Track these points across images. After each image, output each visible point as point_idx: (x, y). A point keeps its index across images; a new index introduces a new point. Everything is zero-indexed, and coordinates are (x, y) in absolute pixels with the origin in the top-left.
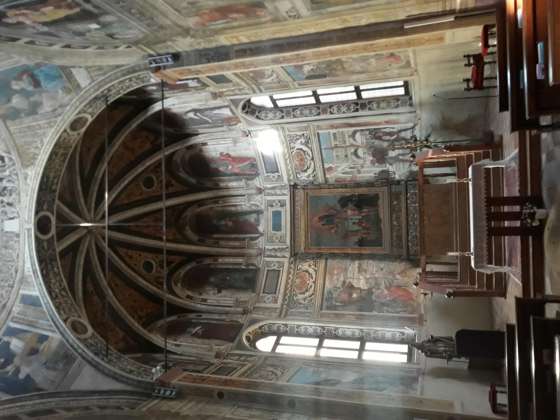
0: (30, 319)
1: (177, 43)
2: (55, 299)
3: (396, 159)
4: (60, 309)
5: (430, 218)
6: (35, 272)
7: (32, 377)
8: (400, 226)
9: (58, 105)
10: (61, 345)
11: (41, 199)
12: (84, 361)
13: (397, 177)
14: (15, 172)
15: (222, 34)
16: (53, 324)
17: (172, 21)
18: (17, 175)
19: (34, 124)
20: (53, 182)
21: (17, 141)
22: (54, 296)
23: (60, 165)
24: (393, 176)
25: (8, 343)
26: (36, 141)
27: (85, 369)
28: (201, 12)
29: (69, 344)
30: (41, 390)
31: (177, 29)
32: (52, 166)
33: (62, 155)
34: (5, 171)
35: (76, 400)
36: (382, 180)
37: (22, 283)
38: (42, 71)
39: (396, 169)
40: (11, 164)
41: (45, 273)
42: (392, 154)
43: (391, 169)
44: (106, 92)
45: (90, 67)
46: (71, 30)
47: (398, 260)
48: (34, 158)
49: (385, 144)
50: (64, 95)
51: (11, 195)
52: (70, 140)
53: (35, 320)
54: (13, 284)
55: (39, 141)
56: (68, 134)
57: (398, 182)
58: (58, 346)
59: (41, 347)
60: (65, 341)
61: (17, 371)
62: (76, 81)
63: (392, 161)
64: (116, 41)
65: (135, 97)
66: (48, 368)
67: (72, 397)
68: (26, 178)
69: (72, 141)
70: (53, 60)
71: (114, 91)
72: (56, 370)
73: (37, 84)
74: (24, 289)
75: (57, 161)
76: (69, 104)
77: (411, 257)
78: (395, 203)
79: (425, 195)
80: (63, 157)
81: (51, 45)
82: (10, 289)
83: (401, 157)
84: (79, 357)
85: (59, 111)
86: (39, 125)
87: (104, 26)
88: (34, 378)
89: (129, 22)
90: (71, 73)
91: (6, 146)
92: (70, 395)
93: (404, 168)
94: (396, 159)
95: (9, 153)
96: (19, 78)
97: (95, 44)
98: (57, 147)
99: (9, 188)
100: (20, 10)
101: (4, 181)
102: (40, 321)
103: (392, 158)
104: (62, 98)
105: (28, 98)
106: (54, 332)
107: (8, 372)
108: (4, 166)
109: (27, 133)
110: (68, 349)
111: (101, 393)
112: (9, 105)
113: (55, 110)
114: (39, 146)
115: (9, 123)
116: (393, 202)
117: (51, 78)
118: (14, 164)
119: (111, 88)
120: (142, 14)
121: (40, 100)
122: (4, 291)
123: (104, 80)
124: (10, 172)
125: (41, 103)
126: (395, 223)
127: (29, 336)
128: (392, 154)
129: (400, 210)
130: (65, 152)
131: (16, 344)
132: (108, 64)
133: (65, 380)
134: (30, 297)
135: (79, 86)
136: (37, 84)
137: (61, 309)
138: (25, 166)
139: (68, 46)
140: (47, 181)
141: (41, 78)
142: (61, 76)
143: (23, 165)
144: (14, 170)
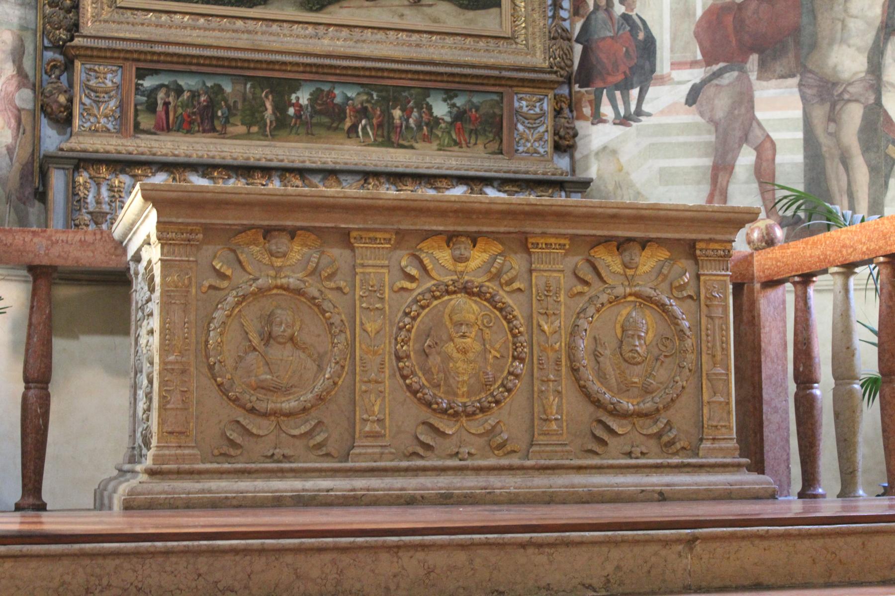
3: (735, 130)
5: (467, 290)
8: (282, 126)
13: (597, 136)
24: (606, 109)
36: (585, 37)
39: (663, 130)
42: (779, 107)
43: (665, 99)
47: (25, 98)
49: (848, 61)
57: (565, 143)
63: (721, 104)
77: (57, 180)
78: (441, 109)
79: (647, 262)
83: (746, 158)
93: (666, 177)
94: (735, 130)
103: (745, 100)
116: (449, 95)
126: (303, 97)
128: (779, 107)
129: (388, 135)
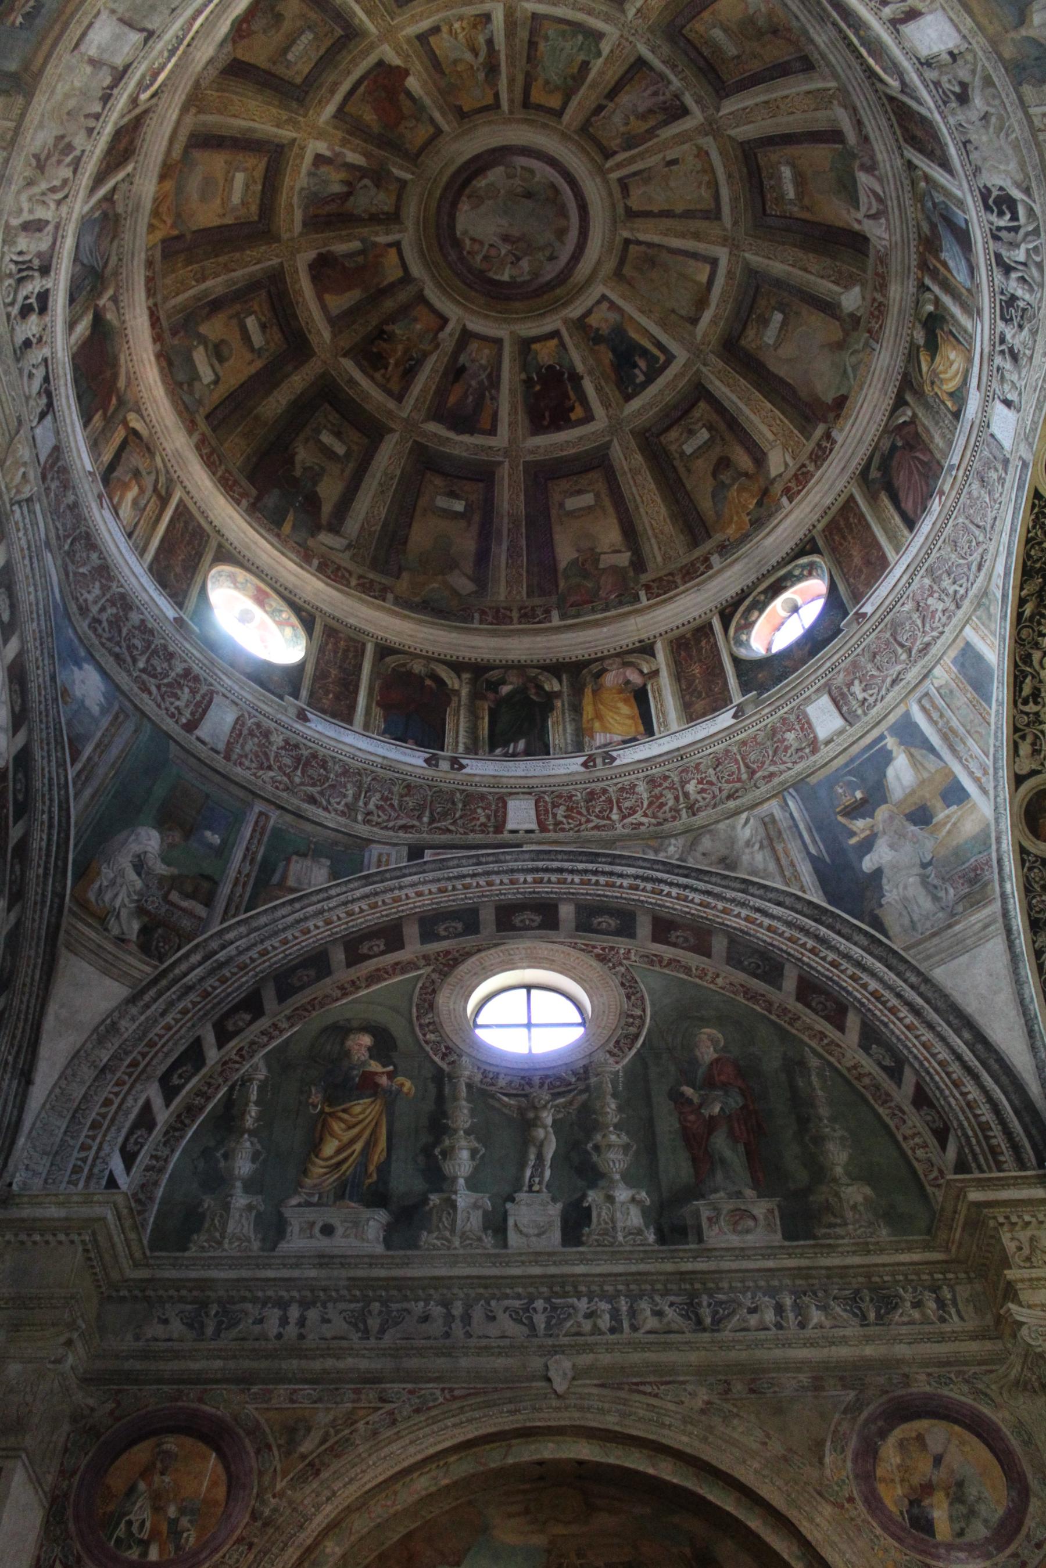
0: (955, 723)
2: (1025, 702)
4: (1023, 738)
6: (1005, 596)
7: (884, 881)
10: (983, 840)
12: (1000, 920)
16: (991, 771)
22: (1027, 690)
25: (887, 757)
27: (989, 945)
29: (998, 850)
30: (878, 924)
35: (917, 1012)
37: (979, 605)
40: (1030, 228)
41: (1027, 613)
53: (961, 730)
54: (963, 597)
58: (974, 838)
59: (941, 816)
60: (993, 835)
61: (867, 845)
66: (924, 881)
67: (921, 995)
72: (936, 899)
74: (975, 629)
82: (953, 607)
84: (996, 907)
88: (886, 888)
92: (923, 988)
102: (970, 742)
106: (985, 791)
107: (853, 834)
108: (1016, 229)
110: (988, 862)
111: (980, 1040)
122: (941, 606)
127: (932, 764)
131: (901, 773)
133: (935, 941)
134: (979, 658)
137: (1029, 739)
144: (1036, 249)
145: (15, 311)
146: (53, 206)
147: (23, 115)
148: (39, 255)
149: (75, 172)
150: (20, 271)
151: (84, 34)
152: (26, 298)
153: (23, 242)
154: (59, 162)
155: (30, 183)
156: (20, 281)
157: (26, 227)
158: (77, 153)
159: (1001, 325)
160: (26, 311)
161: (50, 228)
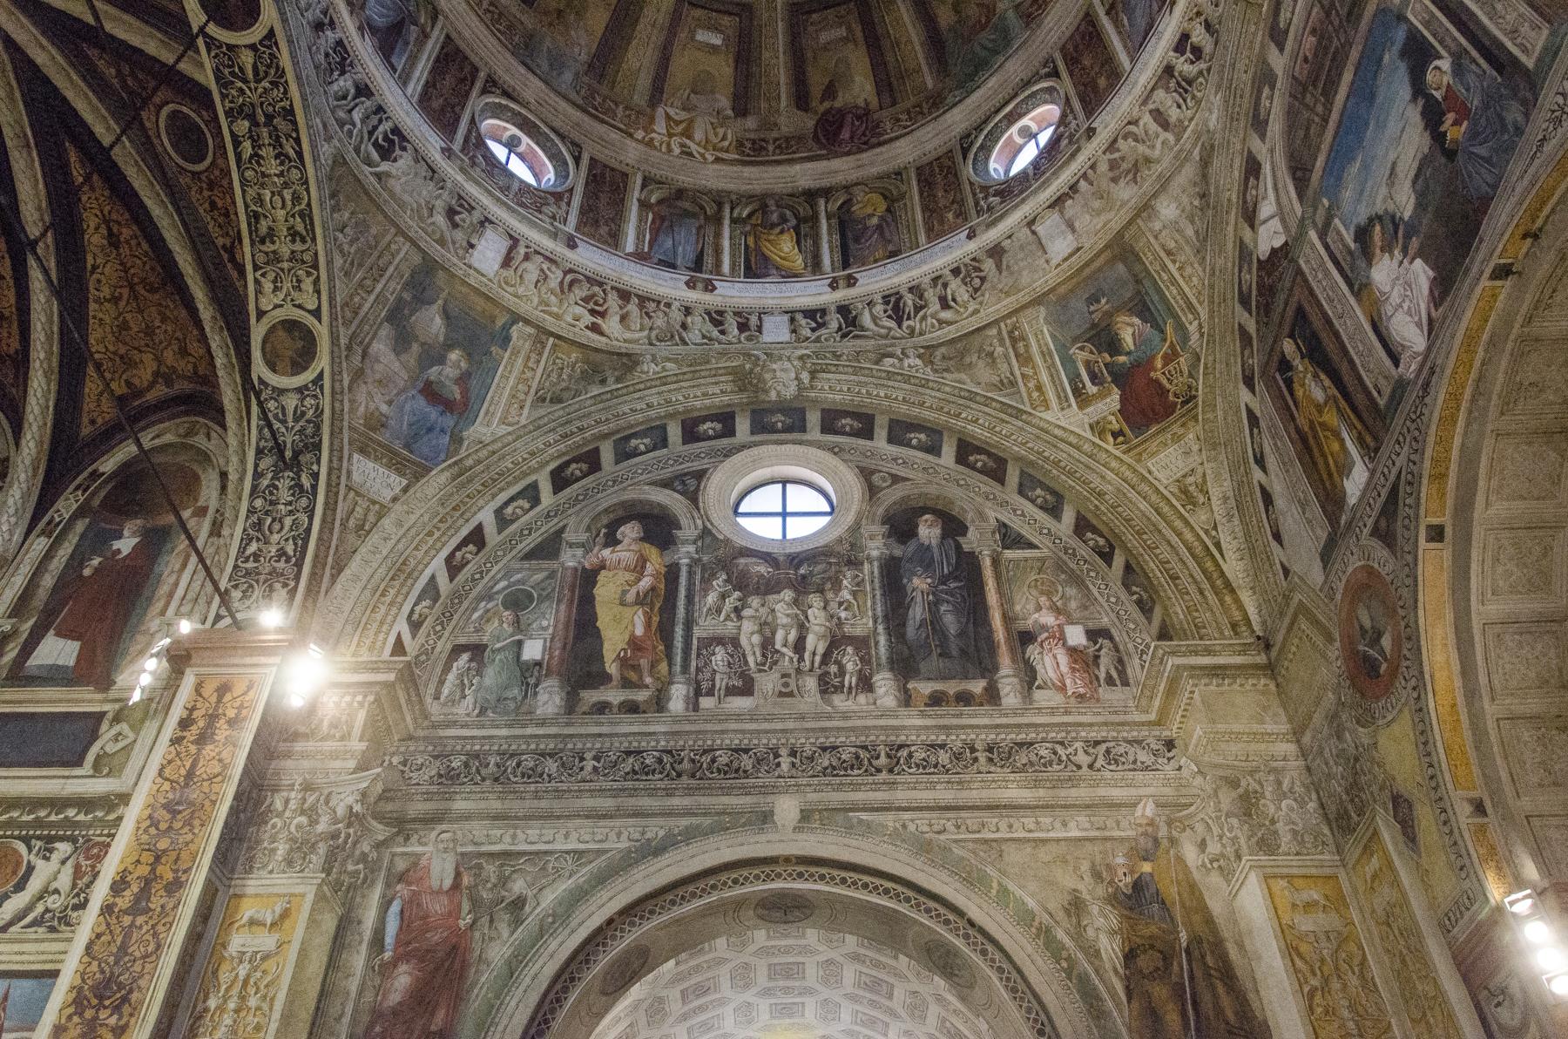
1: (352, 764)
9: (368, 371)
11: (275, 84)
14: (347, 127)
15: (320, 897)
17: (467, 817)
18: (341, 124)
19: (379, 287)
20: (256, 144)
21: (380, 217)
23: (259, 200)
26: (351, 243)
28: (466, 906)
31: (418, 808)
32: (288, 197)
33: (271, 235)
34: (363, 121)
38: (443, 431)
44: (306, 481)
45: (380, 517)
46: (541, 600)
48: (333, 195)
50: (372, 406)
51: (327, 55)
52: (276, 289)
55: (346, 247)
56: (300, 307)
62: (376, 459)
64: (443, 646)
65: (108, 465)
68: (325, 126)
69: (268, 286)
70: (447, 474)
71: (284, 495)
73: (431, 392)
75: (281, 214)
76: (350, 389)
80: (263, 229)
81: (502, 521)
85: (356, 360)
86: (369, 293)
87: (529, 675)
89: (510, 726)
90: (400, 473)
91: (392, 194)
95: (378, 176)
96: (463, 379)
97: (458, 596)
98: (307, 257)
99: (336, 73)
100: (656, 576)
101: (353, 91)
104: (369, 393)
105: (423, 344)
109: (376, 254)
112: (440, 302)
113: (365, 355)
114: (340, 236)
115: (417, 259)
117: (420, 431)
118: (357, 150)
119: (304, 502)
120: (533, 775)
121: (404, 357)
123: (335, 510)
124: (354, 125)
125: (397, 354)
130: (269, 247)
132: (357, 557)
135: (363, 451)
136: (431, 392)
138: (339, 161)
139: (477, 537)
140: (277, 143)
141: (433, 413)
142: (407, 446)
143: (345, 163)
145: (1203, 66)
146: (1141, 123)
147: (1130, 223)
148: (1167, 90)
149: (1115, 141)
150: (1186, 91)
151: (1071, 255)
152: (1192, 63)
153: (1174, 114)
154: (1123, 159)
155: (1148, 160)
156: (1190, 83)
157: (1165, 125)
158: (1109, 156)
159: (339, 35)
160: (1197, 52)
161: (1151, 106)
